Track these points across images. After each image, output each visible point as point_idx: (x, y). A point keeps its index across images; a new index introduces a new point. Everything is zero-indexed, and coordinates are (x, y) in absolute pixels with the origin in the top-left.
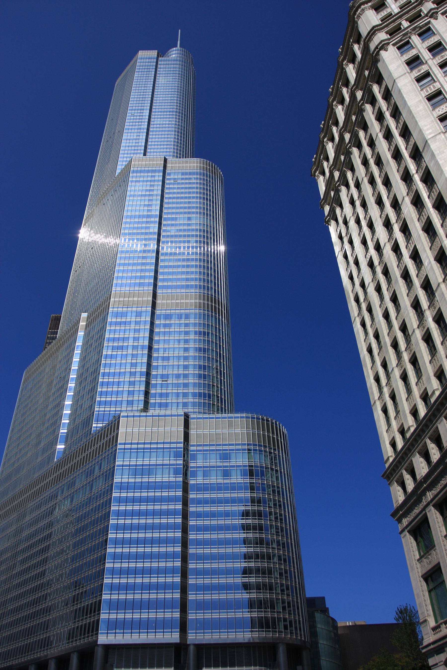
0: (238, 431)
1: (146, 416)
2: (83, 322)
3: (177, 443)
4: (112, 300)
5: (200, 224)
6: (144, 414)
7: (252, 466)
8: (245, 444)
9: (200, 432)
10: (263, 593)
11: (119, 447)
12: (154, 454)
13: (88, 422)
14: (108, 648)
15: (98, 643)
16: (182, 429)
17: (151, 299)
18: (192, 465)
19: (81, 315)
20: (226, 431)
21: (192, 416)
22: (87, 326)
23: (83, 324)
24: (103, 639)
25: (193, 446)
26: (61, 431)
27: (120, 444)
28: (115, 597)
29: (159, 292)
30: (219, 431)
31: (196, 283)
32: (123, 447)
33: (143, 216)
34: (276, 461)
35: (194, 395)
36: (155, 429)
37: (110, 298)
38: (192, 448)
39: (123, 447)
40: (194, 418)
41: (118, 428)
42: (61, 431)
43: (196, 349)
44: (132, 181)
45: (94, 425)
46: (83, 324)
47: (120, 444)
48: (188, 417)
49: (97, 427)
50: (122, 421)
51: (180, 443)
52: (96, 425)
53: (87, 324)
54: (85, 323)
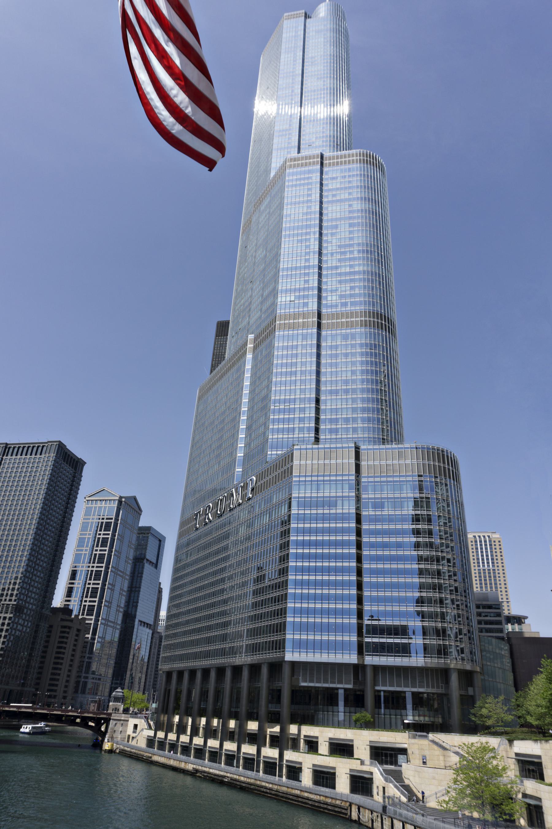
0: (408, 462)
1: (318, 448)
2: (251, 344)
3: (349, 475)
4: (278, 322)
5: (363, 243)
6: (316, 446)
7: (422, 481)
8: (415, 476)
9: (371, 463)
10: (434, 606)
11: (294, 479)
12: (327, 487)
13: (262, 449)
14: (293, 664)
15: (286, 660)
16: (353, 461)
17: (316, 319)
18: (363, 496)
19: (247, 337)
20: (396, 462)
21: (362, 447)
22: (255, 348)
23: (250, 346)
24: (289, 657)
25: (365, 477)
26: (239, 455)
27: (296, 476)
28: (298, 620)
29: (323, 311)
30: (390, 462)
31: (361, 299)
32: (297, 479)
33: (302, 227)
34: (449, 509)
35: (363, 419)
36: (327, 462)
37: (275, 321)
38: (363, 480)
39: (297, 479)
40: (365, 449)
41: (292, 461)
42: (239, 455)
43: (362, 372)
44: (288, 186)
45: (269, 453)
46: (250, 346)
47: (296, 476)
48: (359, 449)
49: (271, 454)
50: (296, 454)
51: (352, 475)
52: (272, 454)
53: (254, 346)
54: (252, 345)
